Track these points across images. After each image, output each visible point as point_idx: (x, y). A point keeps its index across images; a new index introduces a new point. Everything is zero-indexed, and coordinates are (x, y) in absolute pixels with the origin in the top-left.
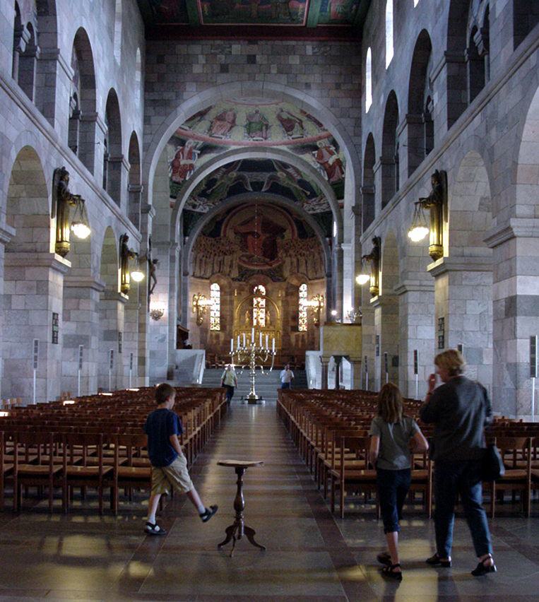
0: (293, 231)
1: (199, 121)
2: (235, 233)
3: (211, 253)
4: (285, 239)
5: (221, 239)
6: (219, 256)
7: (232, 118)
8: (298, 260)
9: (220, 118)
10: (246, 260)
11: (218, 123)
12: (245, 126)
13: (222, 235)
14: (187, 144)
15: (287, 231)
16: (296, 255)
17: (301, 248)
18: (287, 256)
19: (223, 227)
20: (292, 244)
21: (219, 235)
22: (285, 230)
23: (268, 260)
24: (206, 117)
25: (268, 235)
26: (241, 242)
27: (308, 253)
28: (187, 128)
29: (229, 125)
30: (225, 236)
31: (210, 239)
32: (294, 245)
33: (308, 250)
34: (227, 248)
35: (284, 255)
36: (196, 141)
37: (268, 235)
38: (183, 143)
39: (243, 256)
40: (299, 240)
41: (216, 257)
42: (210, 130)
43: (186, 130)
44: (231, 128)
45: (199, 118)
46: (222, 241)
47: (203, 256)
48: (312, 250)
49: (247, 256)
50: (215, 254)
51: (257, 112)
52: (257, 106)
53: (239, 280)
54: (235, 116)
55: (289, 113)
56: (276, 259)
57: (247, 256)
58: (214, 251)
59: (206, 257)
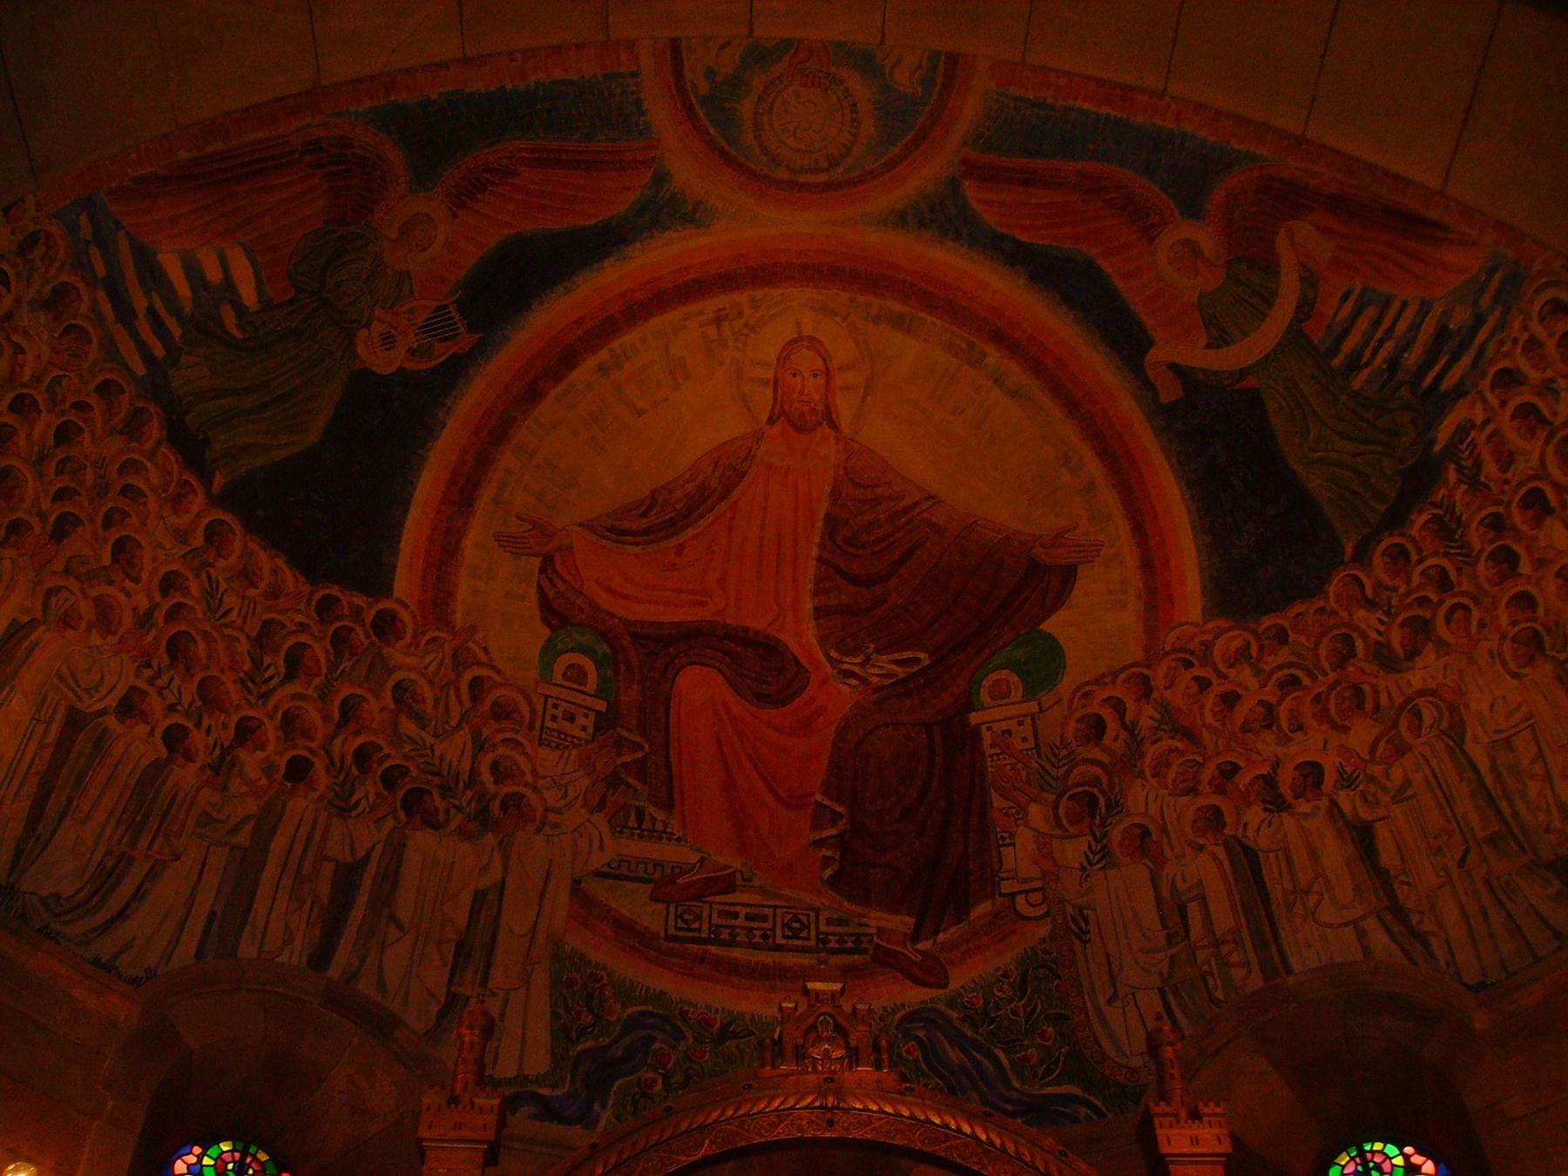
0: (1152, 562)
2: (554, 614)
3: (246, 733)
4: (1067, 683)
5: (386, 626)
6: (342, 806)
8: (1246, 861)
10: (652, 917)
13: (405, 582)
15: (1090, 586)
16: (1213, 820)
17: (1268, 717)
18: (1102, 856)
19: (427, 488)
20: (1147, 717)
21: (376, 581)
22: (1068, 575)
23: (902, 922)
25: (884, 668)
26: (604, 723)
27: (1361, 734)
30: (437, 605)
31: (266, 561)
32: (1171, 721)
33: (1357, 700)
34: (455, 750)
35: (1073, 851)
37: (884, 668)
39: (614, 873)
40: (1233, 640)
41: (301, 806)
46: (396, 654)
47: (129, 707)
48: (1416, 679)
49: (663, 885)
50: (299, 771)
53: (548, 1110)
56: (982, 909)
57: (663, 885)
58: (290, 725)
59: (175, 739)
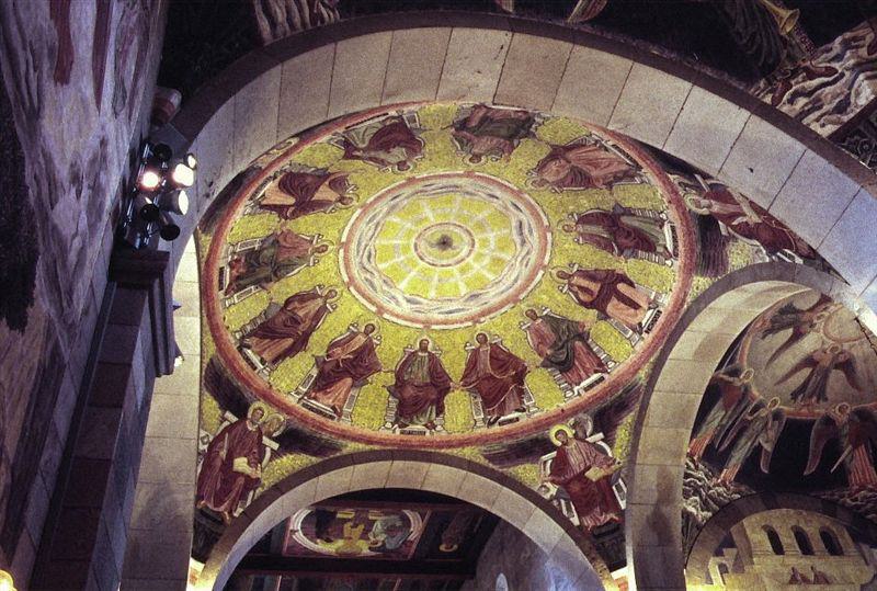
1: (629, 212)
7: (553, 166)
9: (580, 179)
11: (594, 173)
12: (529, 135)
14: (705, 211)
24: (608, 207)
28: (667, 229)
29: (571, 155)
36: (681, 193)
38: (707, 224)
42: (629, 175)
43: (673, 229)
44: (568, 149)
45: (625, 220)
51: (476, 158)
52: (469, 174)
54: (542, 166)
55: (383, 161)
